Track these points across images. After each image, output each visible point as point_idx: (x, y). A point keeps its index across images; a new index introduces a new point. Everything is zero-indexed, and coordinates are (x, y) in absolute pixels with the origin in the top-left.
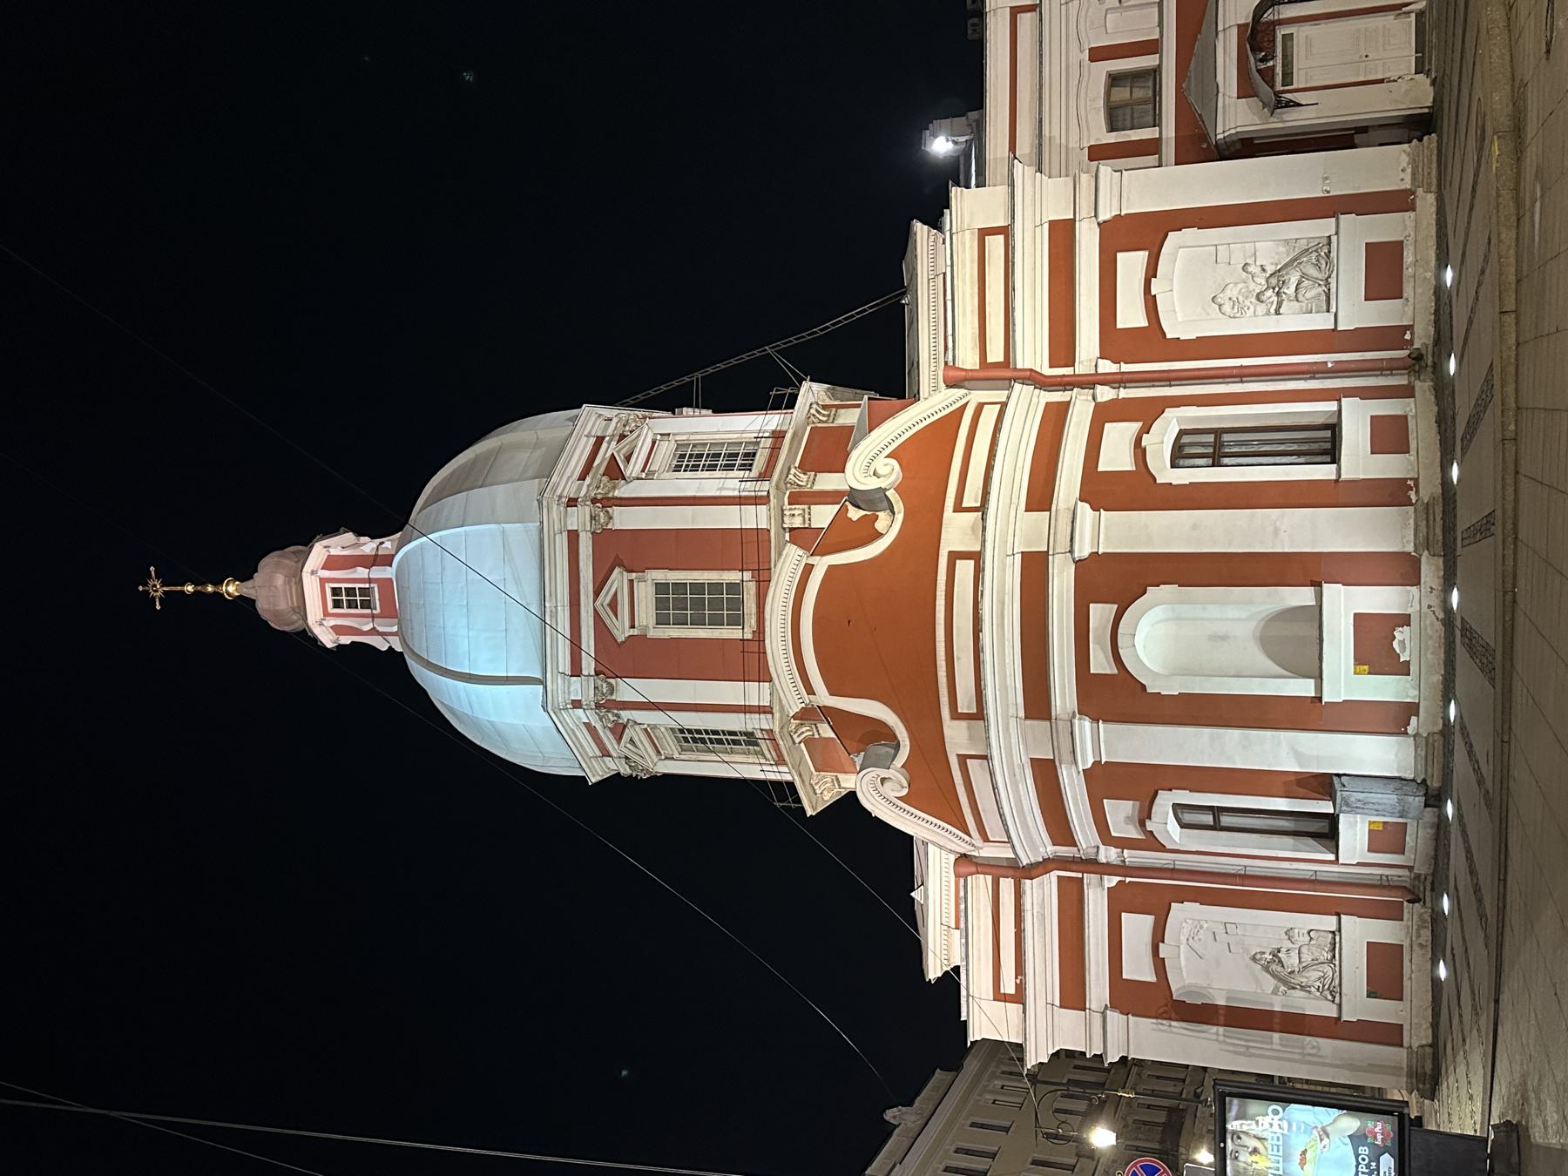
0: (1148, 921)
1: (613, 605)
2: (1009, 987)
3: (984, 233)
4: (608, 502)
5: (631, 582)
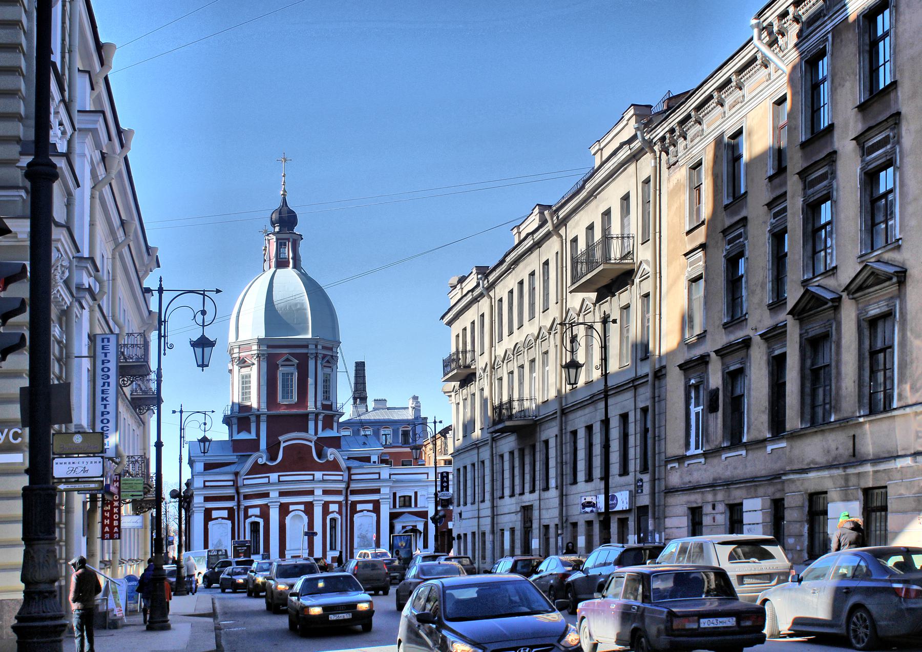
0: (226, 516)
1: (287, 360)
2: (207, 484)
3: (379, 473)
4: (316, 358)
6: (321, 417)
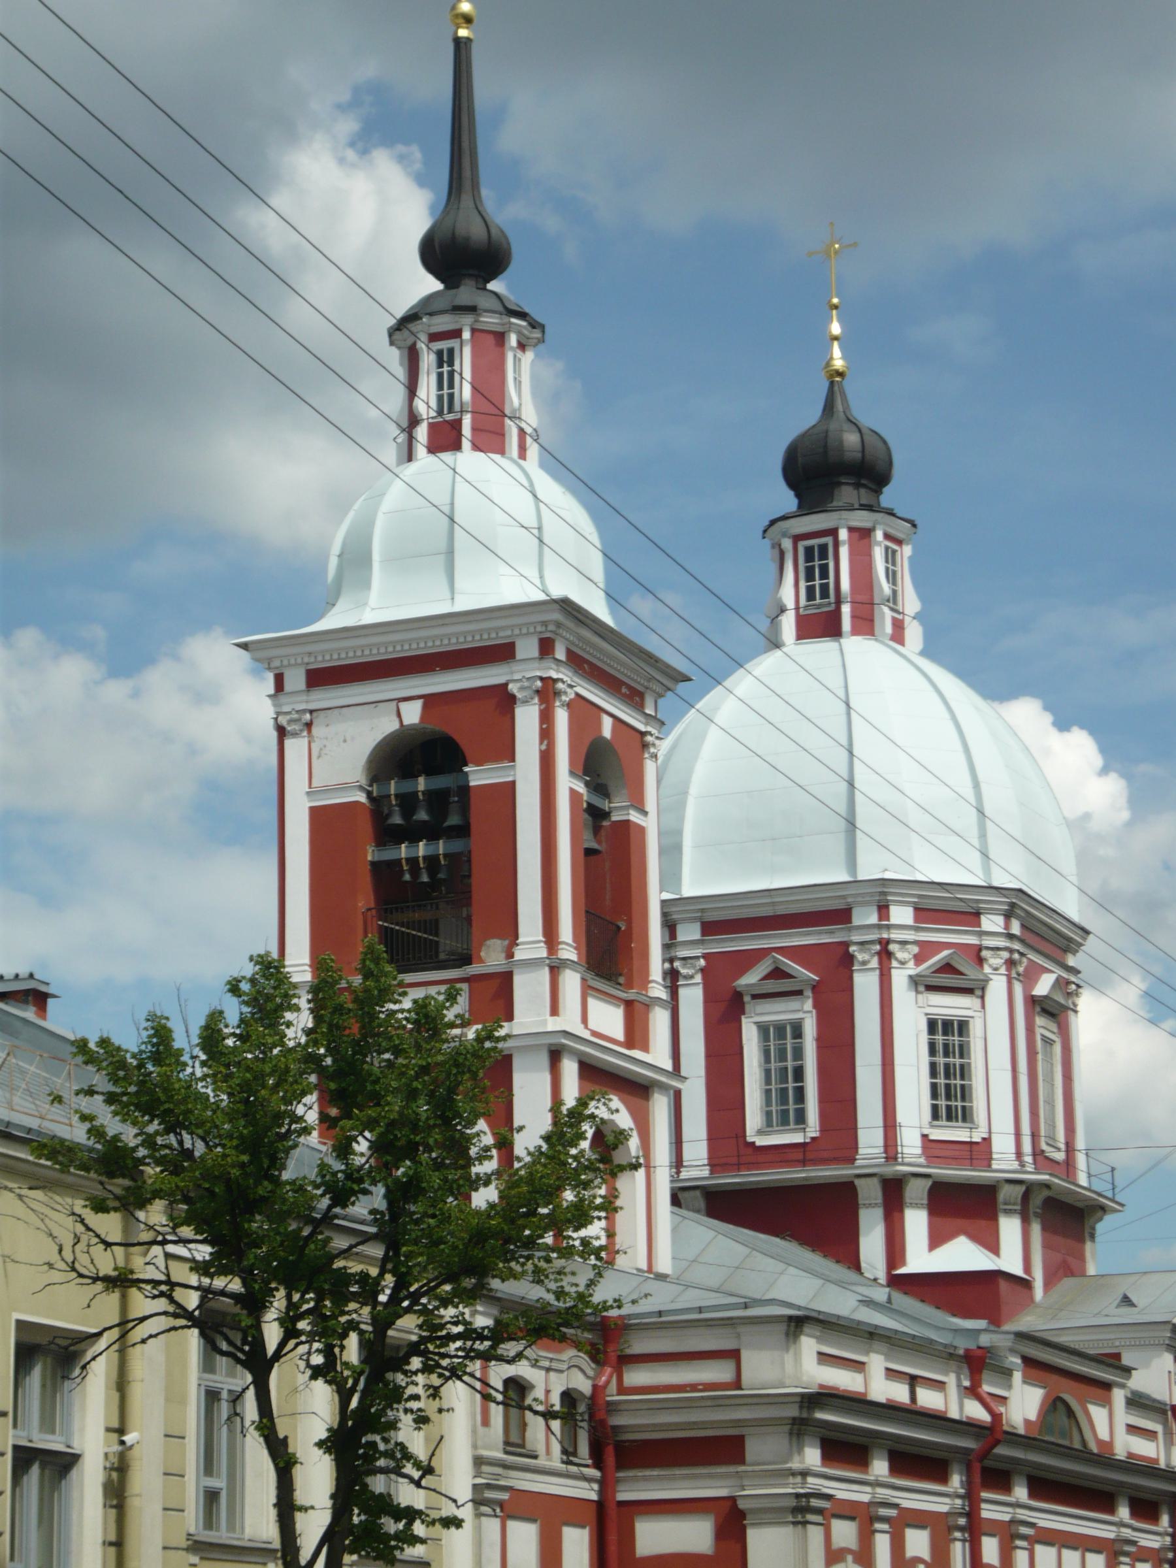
5: (799, 993)
6: (916, 1190)
